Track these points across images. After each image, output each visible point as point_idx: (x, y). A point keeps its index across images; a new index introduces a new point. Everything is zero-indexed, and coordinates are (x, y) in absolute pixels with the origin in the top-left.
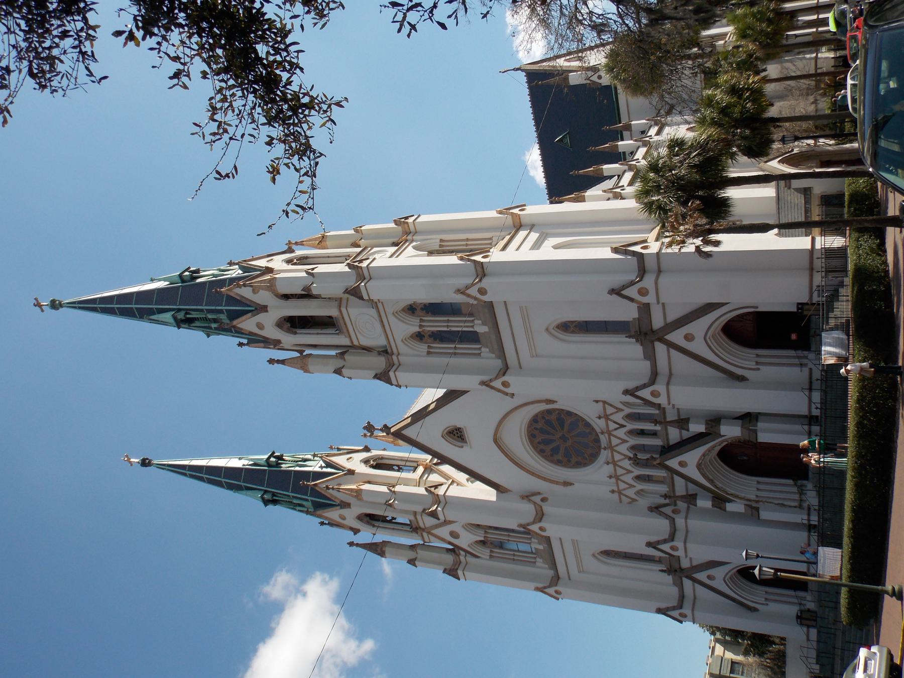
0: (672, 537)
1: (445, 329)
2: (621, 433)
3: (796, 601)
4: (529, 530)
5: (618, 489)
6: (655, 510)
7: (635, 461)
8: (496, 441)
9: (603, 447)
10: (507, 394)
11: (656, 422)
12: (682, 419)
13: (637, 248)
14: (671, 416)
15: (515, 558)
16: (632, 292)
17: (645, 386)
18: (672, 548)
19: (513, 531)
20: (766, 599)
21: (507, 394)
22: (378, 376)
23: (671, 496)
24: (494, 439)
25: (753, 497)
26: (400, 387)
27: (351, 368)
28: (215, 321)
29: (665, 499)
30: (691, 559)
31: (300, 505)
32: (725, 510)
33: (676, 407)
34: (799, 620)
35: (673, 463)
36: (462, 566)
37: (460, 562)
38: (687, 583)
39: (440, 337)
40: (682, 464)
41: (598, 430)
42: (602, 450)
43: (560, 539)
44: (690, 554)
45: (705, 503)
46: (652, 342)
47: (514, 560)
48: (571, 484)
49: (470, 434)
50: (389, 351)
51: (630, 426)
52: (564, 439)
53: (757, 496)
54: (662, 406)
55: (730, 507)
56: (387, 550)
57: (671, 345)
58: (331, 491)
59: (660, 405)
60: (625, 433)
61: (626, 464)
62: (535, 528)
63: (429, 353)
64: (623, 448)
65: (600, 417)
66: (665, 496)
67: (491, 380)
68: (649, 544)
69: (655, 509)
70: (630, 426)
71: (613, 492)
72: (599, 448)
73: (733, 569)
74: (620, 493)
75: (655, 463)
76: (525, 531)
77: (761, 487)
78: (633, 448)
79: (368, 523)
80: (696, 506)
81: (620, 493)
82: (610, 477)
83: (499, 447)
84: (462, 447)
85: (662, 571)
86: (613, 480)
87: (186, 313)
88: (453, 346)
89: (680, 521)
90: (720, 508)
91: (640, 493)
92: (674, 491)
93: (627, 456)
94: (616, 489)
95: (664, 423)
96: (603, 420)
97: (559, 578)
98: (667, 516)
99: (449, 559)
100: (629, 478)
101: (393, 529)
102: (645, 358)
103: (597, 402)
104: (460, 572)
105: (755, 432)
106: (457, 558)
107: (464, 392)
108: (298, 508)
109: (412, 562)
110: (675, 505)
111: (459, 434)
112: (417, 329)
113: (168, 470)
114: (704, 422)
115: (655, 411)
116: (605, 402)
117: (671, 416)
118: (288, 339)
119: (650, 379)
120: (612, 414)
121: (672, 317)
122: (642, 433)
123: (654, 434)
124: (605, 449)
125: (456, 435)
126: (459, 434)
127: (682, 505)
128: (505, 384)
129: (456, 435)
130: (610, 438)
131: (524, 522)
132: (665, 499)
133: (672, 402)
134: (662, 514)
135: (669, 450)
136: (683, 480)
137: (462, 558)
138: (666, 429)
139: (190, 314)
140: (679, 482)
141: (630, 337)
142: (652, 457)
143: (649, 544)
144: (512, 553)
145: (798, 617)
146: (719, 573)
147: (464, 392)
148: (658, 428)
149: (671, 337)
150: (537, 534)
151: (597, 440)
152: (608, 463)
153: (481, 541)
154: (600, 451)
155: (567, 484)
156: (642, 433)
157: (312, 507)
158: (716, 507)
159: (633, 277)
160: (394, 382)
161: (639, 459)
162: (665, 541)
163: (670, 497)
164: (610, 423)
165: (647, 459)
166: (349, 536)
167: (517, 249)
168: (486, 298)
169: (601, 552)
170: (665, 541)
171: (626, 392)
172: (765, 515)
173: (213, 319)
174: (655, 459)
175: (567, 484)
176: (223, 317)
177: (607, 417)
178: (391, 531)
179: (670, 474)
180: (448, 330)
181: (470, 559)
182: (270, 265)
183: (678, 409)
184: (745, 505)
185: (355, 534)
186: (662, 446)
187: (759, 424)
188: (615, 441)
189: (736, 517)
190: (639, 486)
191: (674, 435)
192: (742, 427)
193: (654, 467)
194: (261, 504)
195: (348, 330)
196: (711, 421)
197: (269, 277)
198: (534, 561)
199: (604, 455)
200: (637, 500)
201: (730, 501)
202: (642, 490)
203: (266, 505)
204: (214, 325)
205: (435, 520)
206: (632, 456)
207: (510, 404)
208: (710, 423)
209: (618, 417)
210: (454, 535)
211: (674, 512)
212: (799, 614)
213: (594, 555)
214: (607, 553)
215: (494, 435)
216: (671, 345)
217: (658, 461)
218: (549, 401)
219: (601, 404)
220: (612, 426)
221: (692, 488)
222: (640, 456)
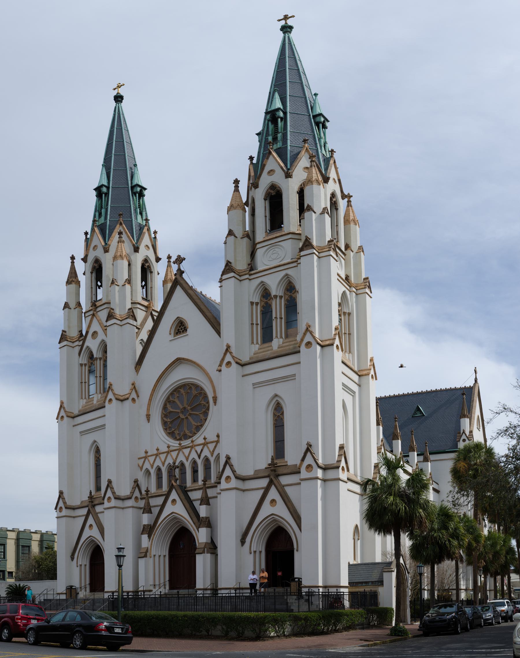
0: (117, 498)
1: (274, 316)
2: (194, 455)
3: (83, 585)
4: (108, 391)
5: (148, 456)
6: (136, 484)
7: (173, 467)
9: (182, 442)
10: (220, 365)
11: (205, 481)
12: (208, 500)
13: (343, 464)
14: (211, 493)
15: (83, 384)
17: (234, 471)
18: (109, 498)
19: (105, 379)
20: (81, 565)
21: (220, 365)
22: (230, 264)
23: (148, 496)
24: (180, 358)
25: (153, 553)
26: (220, 282)
27: (235, 244)
28: (275, 139)
29: (145, 491)
30: (103, 512)
32: (142, 534)
33: (219, 496)
34: (69, 587)
35: (174, 495)
36: (71, 344)
37: (73, 342)
38: (84, 511)
40: (174, 501)
41: (194, 438)
42: (178, 442)
43: (104, 416)
44: (106, 512)
45: (146, 519)
46: (268, 476)
47: (82, 383)
48: (149, 420)
49: (182, 341)
50: (252, 272)
51: (199, 462)
53: (155, 556)
54: (218, 486)
55: (145, 537)
56: (73, 286)
59: (220, 483)
61: (170, 461)
62: (110, 396)
63: (252, 303)
64: (181, 458)
65: (205, 439)
66: (147, 491)
67: (231, 353)
68: (110, 482)
69: (136, 484)
70: (199, 462)
71: (146, 452)
72: (180, 439)
73: (100, 542)
74: (145, 458)
75: (173, 482)
76: (106, 389)
77: (162, 557)
78: (182, 464)
79: (94, 268)
80: (143, 513)
81: (145, 458)
82: (158, 450)
83: (174, 362)
84: (170, 334)
85: (91, 493)
86: (155, 452)
87: (282, 119)
88: (259, 322)
89: (130, 503)
90: (143, 530)
91: (148, 472)
92: (152, 497)
93: (176, 461)
94: (149, 454)
95: (205, 488)
96: (202, 441)
97: (73, 418)
98: (132, 493)
99: (74, 333)
100: (158, 463)
101: (92, 288)
102: (256, 471)
103: (218, 436)
104: (65, 343)
105: (203, 552)
106: (77, 339)
107: (219, 333)
108: (97, 214)
109: (66, 306)
110: (141, 499)
111: (181, 331)
112: (273, 293)
113: (114, 115)
114: (207, 516)
115: (213, 479)
116: (217, 442)
117: (211, 493)
118: (259, 194)
119: (239, 475)
120: (208, 448)
121: (289, 490)
122: (195, 471)
123: (195, 480)
124: (180, 444)
125: (180, 328)
126: (181, 331)
127: (142, 504)
128: (229, 364)
129: (180, 328)
130: (189, 447)
131: (114, 387)
132: (145, 491)
133: (222, 493)
134: (134, 488)
135: (184, 492)
136: (161, 503)
137: (77, 343)
138: (199, 489)
139: (281, 121)
140: (160, 501)
141: (272, 459)
142: (177, 480)
143: (110, 482)
144: (87, 381)
145: (71, 587)
146: (95, 533)
147: (219, 333)
148: (200, 482)
150: (106, 397)
152: (168, 447)
153: (93, 355)
154: (178, 440)
155: (148, 417)
156: (195, 471)
157: (100, 224)
158: (144, 527)
159: (320, 461)
160: (224, 277)
161: (175, 469)
162: (114, 493)
163: (147, 494)
164: (201, 447)
165: (175, 476)
166: (80, 254)
167: (342, 373)
169: (98, 447)
170: (114, 493)
171: (228, 458)
172: (142, 562)
173: (277, 138)
174: (176, 482)
175: (148, 417)
176: (279, 145)
177: (205, 444)
178: (90, 287)
179: (166, 493)
180: (273, 318)
181: (77, 349)
182: (331, 181)
183: (216, 497)
184: (148, 547)
185: (82, 259)
186: (186, 486)
187: (209, 555)
188: (186, 451)
189: (139, 543)
190: (153, 471)
191: (196, 495)
192: (206, 543)
193: (169, 481)
194: (96, 186)
195: (270, 239)
196: (209, 520)
197: (320, 180)
198: (83, 397)
199: (175, 444)
200: (141, 470)
201: (149, 537)
202: (150, 474)
203: (95, 189)
204: (270, 139)
205: (106, 319)
206: (176, 464)
207: (212, 369)
208: (208, 520)
209: (206, 453)
210: (95, 333)
211: (136, 498)
212: (73, 587)
213: (95, 441)
214: (98, 451)
215: (183, 358)
217: (174, 484)
219: (216, 439)
220: (199, 449)
221: (156, 511)
222: (177, 470)
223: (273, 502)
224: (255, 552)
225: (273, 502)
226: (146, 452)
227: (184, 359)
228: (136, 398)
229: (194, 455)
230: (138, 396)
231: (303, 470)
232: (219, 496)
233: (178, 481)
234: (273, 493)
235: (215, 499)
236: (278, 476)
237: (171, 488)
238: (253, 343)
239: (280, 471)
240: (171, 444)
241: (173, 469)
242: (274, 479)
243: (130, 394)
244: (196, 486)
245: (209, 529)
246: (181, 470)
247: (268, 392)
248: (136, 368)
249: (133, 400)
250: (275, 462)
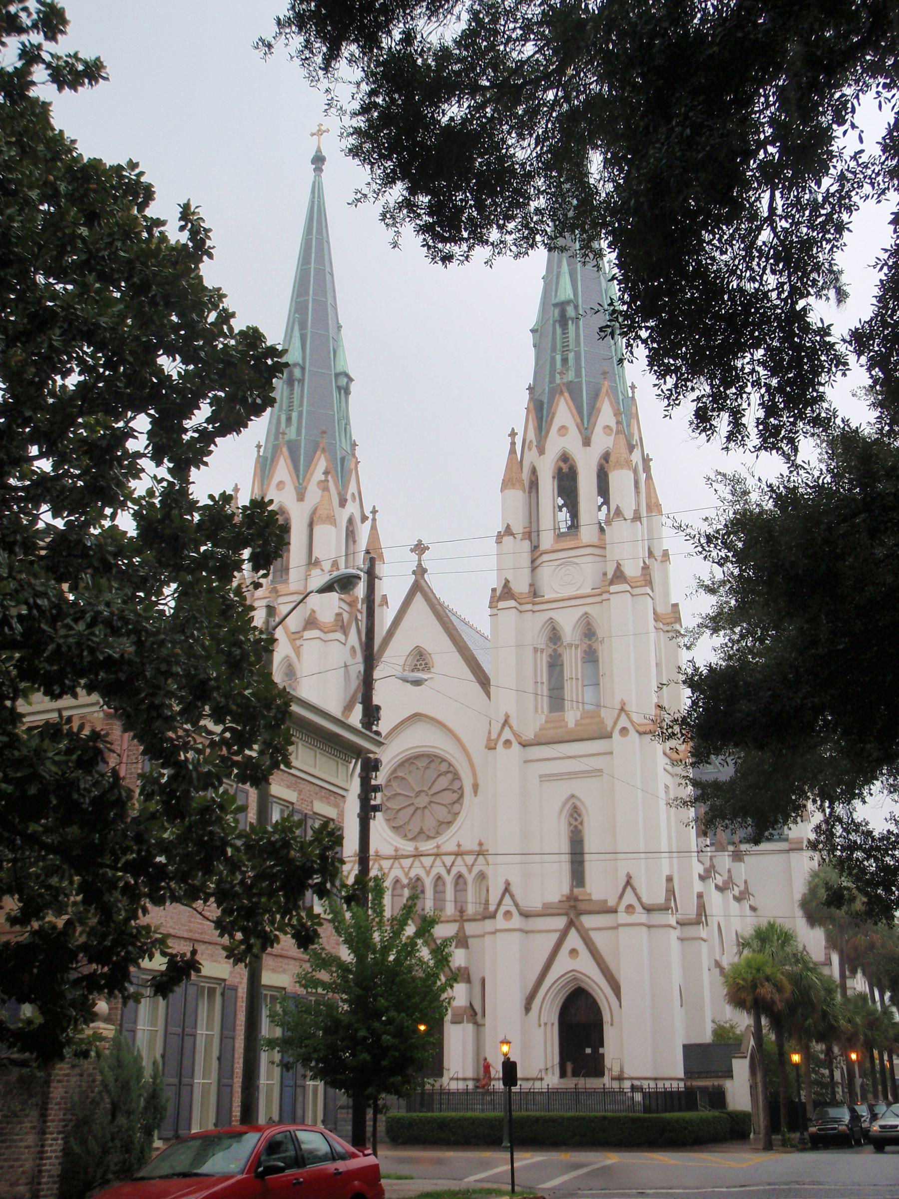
8: (416, 715)
14: (470, 928)
16: (629, 898)
39: (555, 665)
51: (449, 880)
57: (564, 934)
70: (449, 880)
117: (470, 928)
125: (418, 663)
129: (418, 663)
149: (573, 933)
216: (564, 934)
218: (476, 787)
223: (574, 952)
224: (546, 1024)
225: (574, 952)
227: (426, 716)
229: (439, 869)
234: (573, 940)
236: (580, 913)
238: (536, 711)
239: (583, 906)
240: (399, 846)
245: (468, 985)
247: (561, 791)
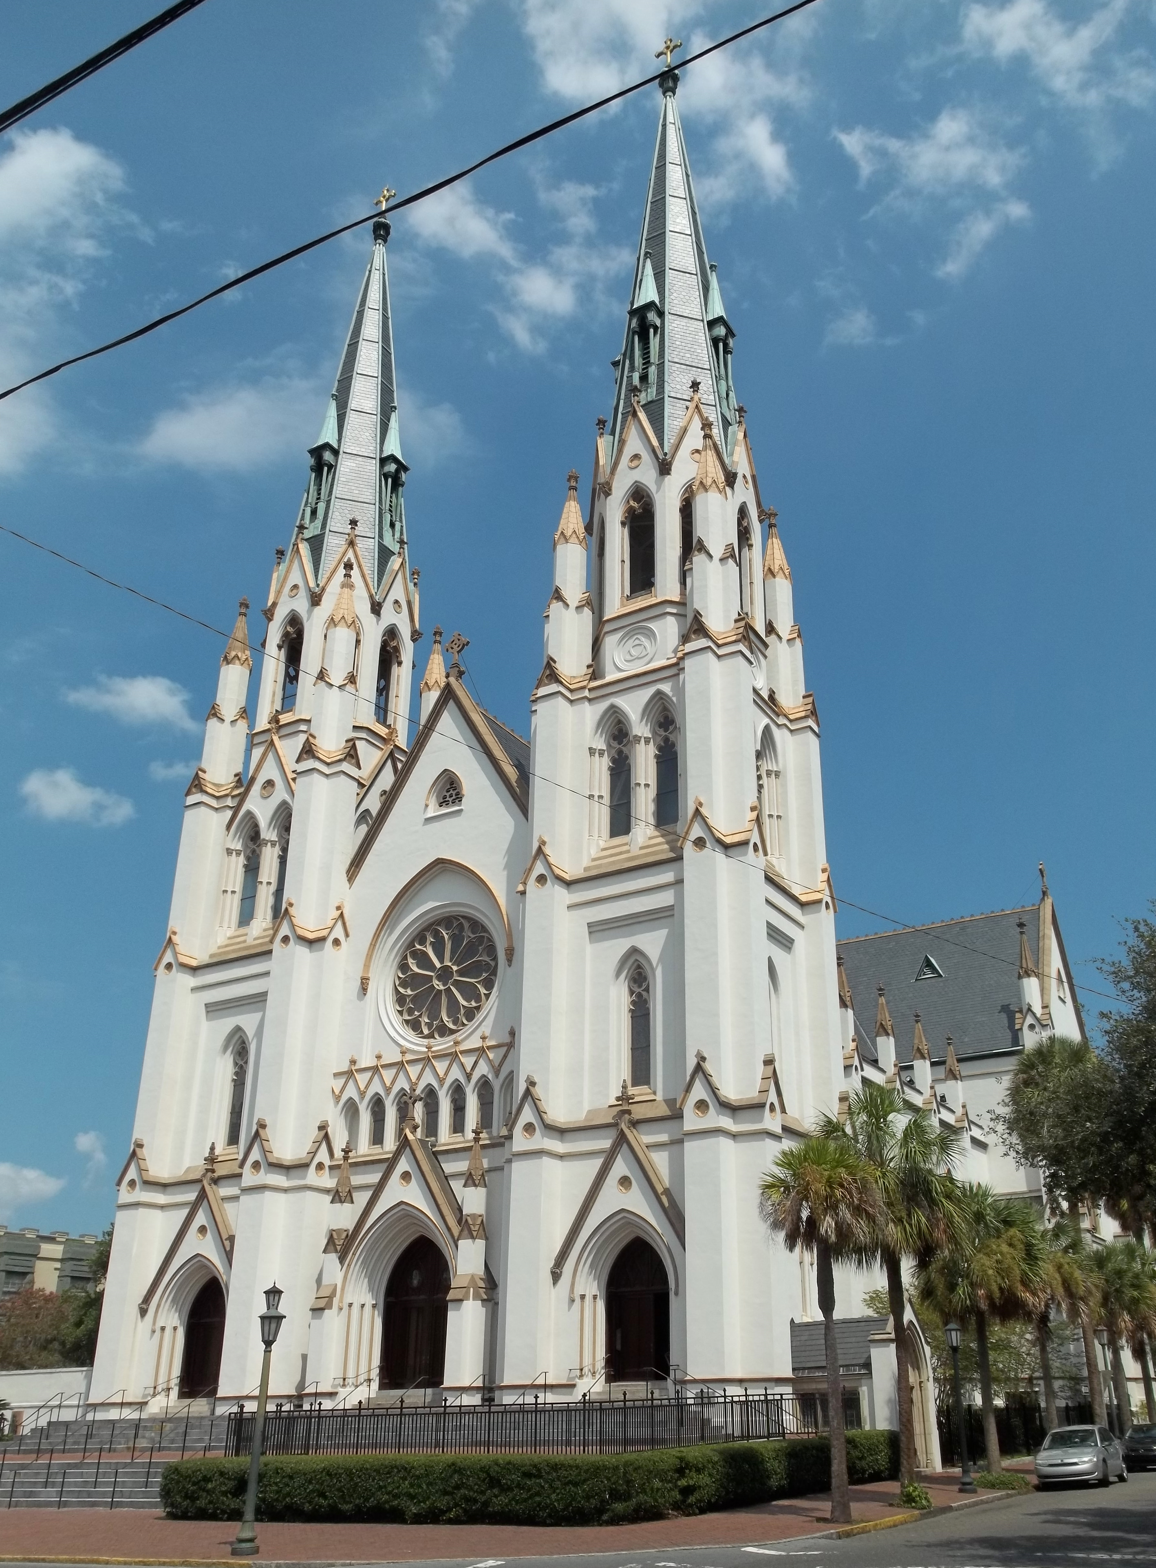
7: (411, 1098)
16: (699, 1092)
31: (314, 512)
52: (445, 974)
58: (341, 571)
59: (510, 1137)
60: (457, 1080)
61: (402, 1083)
75: (407, 1131)
82: (379, 1057)
100: (376, 1087)
142: (415, 1127)
151: (444, 1031)
168: (689, 850)
193: (400, 1132)
199: (415, 1043)
206: (418, 1092)
217: (410, 1137)
226: (353, 1062)
228: (342, 938)
230: (347, 935)
231: (689, 1110)
232: (506, 1166)
233: (419, 1130)
235: (498, 1173)
237: (404, 1144)
241: (410, 1101)
242: (627, 1131)
243: (332, 928)
244: (458, 1141)
246: (426, 1105)
248: (348, 871)
249: (337, 942)
250: (630, 1093)
